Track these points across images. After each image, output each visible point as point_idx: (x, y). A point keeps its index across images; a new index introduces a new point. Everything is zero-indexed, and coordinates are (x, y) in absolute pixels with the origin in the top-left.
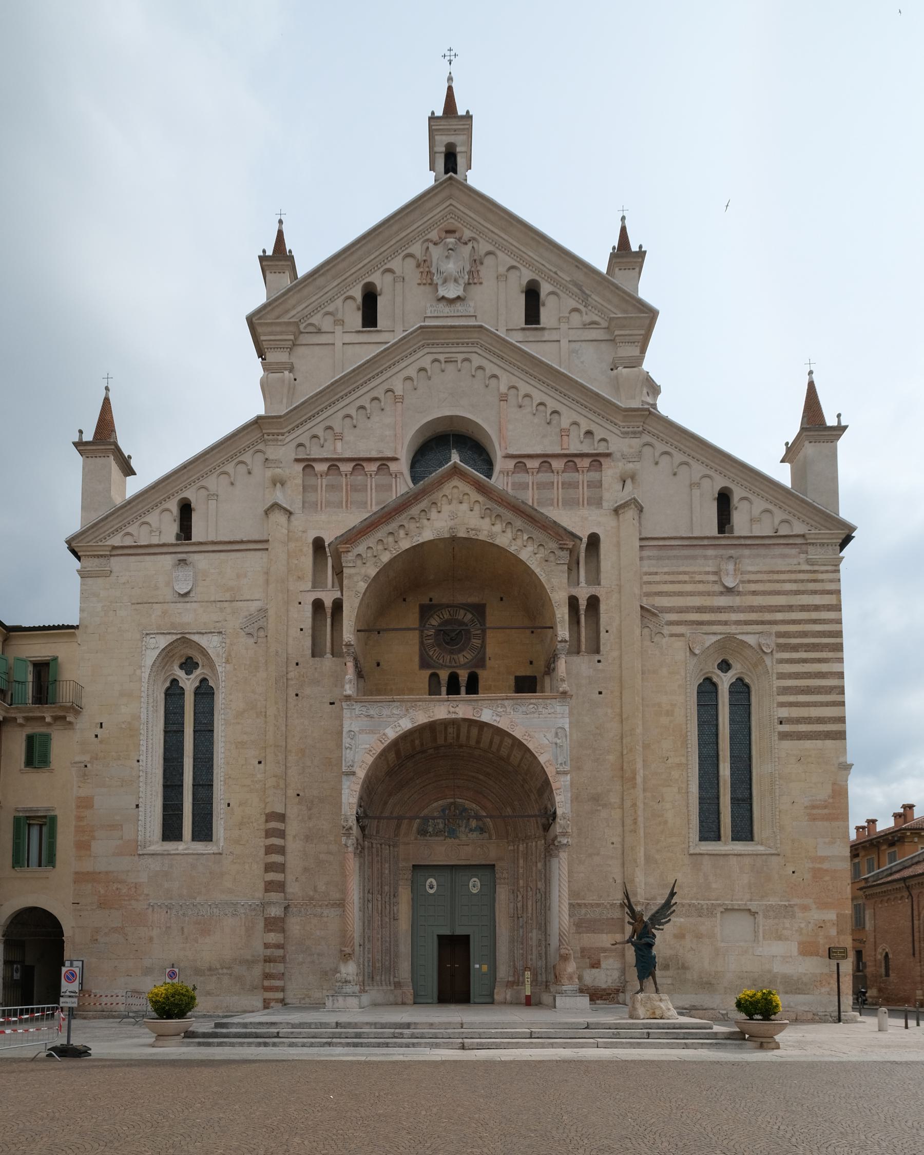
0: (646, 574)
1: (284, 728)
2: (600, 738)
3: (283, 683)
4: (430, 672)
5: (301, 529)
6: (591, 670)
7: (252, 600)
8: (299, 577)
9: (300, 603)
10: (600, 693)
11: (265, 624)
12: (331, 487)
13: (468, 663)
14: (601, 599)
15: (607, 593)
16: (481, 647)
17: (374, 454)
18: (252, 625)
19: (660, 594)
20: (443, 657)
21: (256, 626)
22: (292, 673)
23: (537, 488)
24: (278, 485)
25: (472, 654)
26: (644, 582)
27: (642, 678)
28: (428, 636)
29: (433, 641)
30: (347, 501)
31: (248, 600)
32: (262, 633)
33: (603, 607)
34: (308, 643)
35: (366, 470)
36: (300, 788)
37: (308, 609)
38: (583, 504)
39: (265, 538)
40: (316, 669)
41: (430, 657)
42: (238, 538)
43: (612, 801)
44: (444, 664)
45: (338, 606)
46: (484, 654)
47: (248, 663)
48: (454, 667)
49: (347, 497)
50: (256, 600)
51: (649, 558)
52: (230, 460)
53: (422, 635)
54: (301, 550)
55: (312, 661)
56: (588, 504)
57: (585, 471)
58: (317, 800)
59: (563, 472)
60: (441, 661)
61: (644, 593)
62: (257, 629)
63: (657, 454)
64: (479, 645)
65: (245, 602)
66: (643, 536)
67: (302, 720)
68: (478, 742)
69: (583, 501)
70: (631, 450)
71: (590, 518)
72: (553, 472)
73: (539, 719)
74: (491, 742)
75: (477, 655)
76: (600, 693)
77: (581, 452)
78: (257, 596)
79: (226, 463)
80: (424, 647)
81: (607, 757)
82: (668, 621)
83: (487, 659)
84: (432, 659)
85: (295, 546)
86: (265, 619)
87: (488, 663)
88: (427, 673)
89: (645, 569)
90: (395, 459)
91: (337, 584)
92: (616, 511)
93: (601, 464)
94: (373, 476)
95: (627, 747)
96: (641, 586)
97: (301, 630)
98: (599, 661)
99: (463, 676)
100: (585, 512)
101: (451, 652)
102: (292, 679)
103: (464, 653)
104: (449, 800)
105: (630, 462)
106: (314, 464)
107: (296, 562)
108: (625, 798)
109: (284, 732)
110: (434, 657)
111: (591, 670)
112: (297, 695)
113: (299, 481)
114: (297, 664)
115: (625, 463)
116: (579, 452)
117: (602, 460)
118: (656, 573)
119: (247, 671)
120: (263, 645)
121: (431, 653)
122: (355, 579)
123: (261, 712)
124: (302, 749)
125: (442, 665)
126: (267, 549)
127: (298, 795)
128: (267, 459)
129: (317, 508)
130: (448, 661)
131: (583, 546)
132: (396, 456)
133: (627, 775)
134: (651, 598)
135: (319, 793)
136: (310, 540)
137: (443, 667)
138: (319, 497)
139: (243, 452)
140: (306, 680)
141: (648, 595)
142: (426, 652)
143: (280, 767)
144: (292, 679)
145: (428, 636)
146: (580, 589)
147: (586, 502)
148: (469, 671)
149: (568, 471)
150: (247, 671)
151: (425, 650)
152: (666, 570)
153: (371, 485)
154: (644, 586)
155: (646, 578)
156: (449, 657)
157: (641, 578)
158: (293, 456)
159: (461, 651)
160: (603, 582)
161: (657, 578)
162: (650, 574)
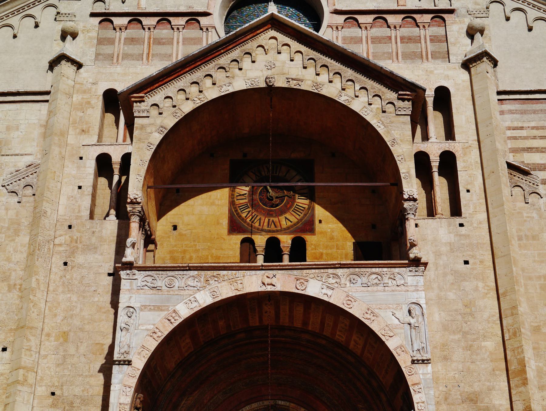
0: (509, 128)
1: (42, 305)
2: (471, 318)
3: (49, 249)
4: (241, 237)
5: (91, 80)
6: (452, 235)
7: (21, 155)
8: (83, 131)
9: (81, 158)
10: (466, 262)
11: (35, 180)
12: (131, 41)
13: (292, 226)
14: (457, 155)
15: (463, 148)
16: (309, 209)
17: (183, 9)
18: (18, 182)
19: (529, 150)
20: (260, 219)
21: (23, 183)
22: (62, 238)
23: (372, 42)
24: (69, 38)
25: (297, 216)
26: (508, 137)
27: (520, 246)
28: (240, 195)
29: (247, 201)
30: (148, 54)
31: (17, 155)
32: (29, 191)
33: (460, 165)
34: (87, 202)
35: (172, 24)
36: (57, 384)
37: (91, 166)
38: (427, 59)
39: (47, 89)
40: (93, 232)
41: (243, 219)
42: (13, 89)
43: (497, 402)
44: (261, 227)
45: (126, 158)
46: (313, 216)
47: (6, 225)
48: (273, 231)
49: (149, 49)
50: (26, 155)
51: (511, 112)
52: (16, 13)
53: (233, 195)
54: (89, 103)
55: (89, 223)
56: (432, 57)
57: (426, 26)
58: (78, 401)
59: (400, 27)
60: (257, 225)
61: (510, 149)
62: (23, 186)
63: (508, 10)
64: (306, 206)
65: (13, 157)
66: (501, 89)
67: (69, 295)
68: (305, 323)
69: (427, 55)
70: (478, 7)
71: (435, 72)
72: (389, 27)
73: (385, 293)
74: (322, 323)
75: (303, 217)
76: (466, 262)
77: (420, 8)
78: (29, 150)
79: (11, 16)
80: (235, 208)
81: (483, 344)
82: (543, 180)
83: (317, 222)
84: (245, 222)
85: (83, 98)
86: (35, 174)
87: (318, 227)
88: (238, 238)
89: (508, 124)
90: (206, 14)
91: (128, 139)
92: (466, 65)
93: (444, 20)
94: (180, 30)
95: (509, 330)
96: (505, 141)
97: (80, 187)
98: (461, 225)
99: (286, 241)
100: (430, 65)
101: (269, 214)
102: (60, 245)
103: (287, 215)
104: (266, 403)
105: (477, 17)
106: (112, 18)
107: (82, 114)
108: (513, 400)
109: (43, 310)
110: (248, 220)
111: (452, 235)
112: (65, 264)
113: (94, 34)
114: (70, 227)
115: (472, 18)
116: (417, 8)
117: (445, 16)
118: (522, 128)
119: (4, 235)
120: (28, 205)
121: (244, 215)
122: (149, 130)
123: (15, 285)
124: (65, 333)
125: (258, 229)
126: (47, 101)
127: (53, 394)
128: (58, 13)
129: (113, 60)
130: (266, 224)
131: (430, 101)
132: (208, 11)
133: (513, 368)
134: (518, 155)
135: (83, 391)
136: (101, 92)
137: (261, 231)
138: (116, 50)
139: (32, 6)
140: (80, 246)
141: (514, 151)
142: (238, 214)
143: (32, 355)
144: (60, 245)
145: (240, 195)
146: (430, 145)
147: (430, 56)
148: (293, 236)
149: (406, 26)
150: (4, 235)
151: (236, 211)
152: (533, 124)
153: (178, 39)
154: (509, 141)
155: (509, 133)
156: (267, 220)
157: (504, 133)
158: (90, 11)
159: (282, 212)
160: (457, 137)
161: (524, 133)
162: (515, 129)
